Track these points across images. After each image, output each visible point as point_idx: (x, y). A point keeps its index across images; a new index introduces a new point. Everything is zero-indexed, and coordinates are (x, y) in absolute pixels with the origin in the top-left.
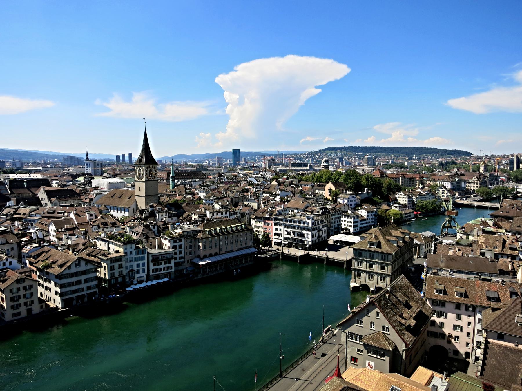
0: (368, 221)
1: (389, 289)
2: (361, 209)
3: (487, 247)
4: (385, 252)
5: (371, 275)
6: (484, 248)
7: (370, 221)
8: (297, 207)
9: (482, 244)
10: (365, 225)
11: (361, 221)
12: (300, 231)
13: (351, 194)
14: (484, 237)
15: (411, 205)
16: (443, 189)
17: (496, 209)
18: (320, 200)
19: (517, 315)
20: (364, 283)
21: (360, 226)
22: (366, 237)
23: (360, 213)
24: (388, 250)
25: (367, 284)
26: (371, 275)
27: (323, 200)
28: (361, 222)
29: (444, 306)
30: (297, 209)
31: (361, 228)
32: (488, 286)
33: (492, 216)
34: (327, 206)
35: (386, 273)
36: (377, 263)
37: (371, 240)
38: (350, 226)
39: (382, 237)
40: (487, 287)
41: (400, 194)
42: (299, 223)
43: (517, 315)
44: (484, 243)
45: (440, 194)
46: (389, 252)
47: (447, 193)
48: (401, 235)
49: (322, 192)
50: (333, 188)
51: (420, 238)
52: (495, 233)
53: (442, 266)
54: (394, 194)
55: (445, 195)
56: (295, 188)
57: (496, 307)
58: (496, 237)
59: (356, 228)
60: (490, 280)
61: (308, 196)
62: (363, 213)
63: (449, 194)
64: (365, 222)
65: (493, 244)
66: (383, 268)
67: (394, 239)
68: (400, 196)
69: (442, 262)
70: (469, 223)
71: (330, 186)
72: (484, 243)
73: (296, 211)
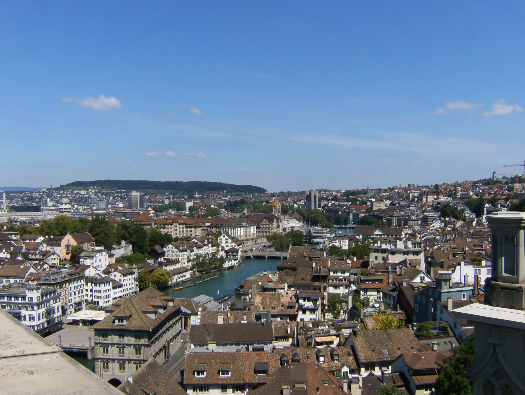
0: (126, 287)
1: (131, 380)
2: (115, 271)
3: (264, 308)
4: (138, 329)
5: (122, 363)
6: (261, 309)
7: (128, 287)
8: (15, 274)
9: (260, 305)
10: (121, 294)
11: (114, 288)
12: (16, 310)
13: (100, 251)
14: (260, 295)
15: (186, 261)
16: (226, 237)
17: (285, 258)
18: (54, 262)
19: (283, 387)
20: (114, 377)
21: (114, 296)
22: (113, 311)
23: (113, 278)
24: (142, 327)
25: (117, 378)
26: (122, 363)
27: (57, 261)
28: (116, 290)
29: (208, 391)
30: (15, 277)
31: (115, 298)
32: (257, 358)
33: (280, 269)
34: (62, 270)
35: (141, 358)
36: (129, 345)
37: (119, 315)
38: (97, 297)
39: (134, 309)
40: (257, 359)
41: (170, 246)
42: (17, 297)
43: (283, 387)
44: (260, 303)
45: (223, 244)
46: (144, 329)
47: (231, 243)
48: (160, 304)
49: (57, 249)
50: (74, 243)
51: (192, 305)
52: (274, 290)
53: (208, 339)
54: (163, 246)
55: (229, 245)
56: (13, 246)
57: (262, 382)
58: (274, 295)
59: (108, 299)
60: (262, 349)
61: (34, 257)
62: (116, 276)
63: (234, 244)
64: (121, 289)
65: (271, 303)
66: (138, 352)
67: (151, 309)
68: (170, 249)
69: (209, 334)
70: (249, 279)
71: (69, 240)
72: (260, 303)
73: (12, 281)
